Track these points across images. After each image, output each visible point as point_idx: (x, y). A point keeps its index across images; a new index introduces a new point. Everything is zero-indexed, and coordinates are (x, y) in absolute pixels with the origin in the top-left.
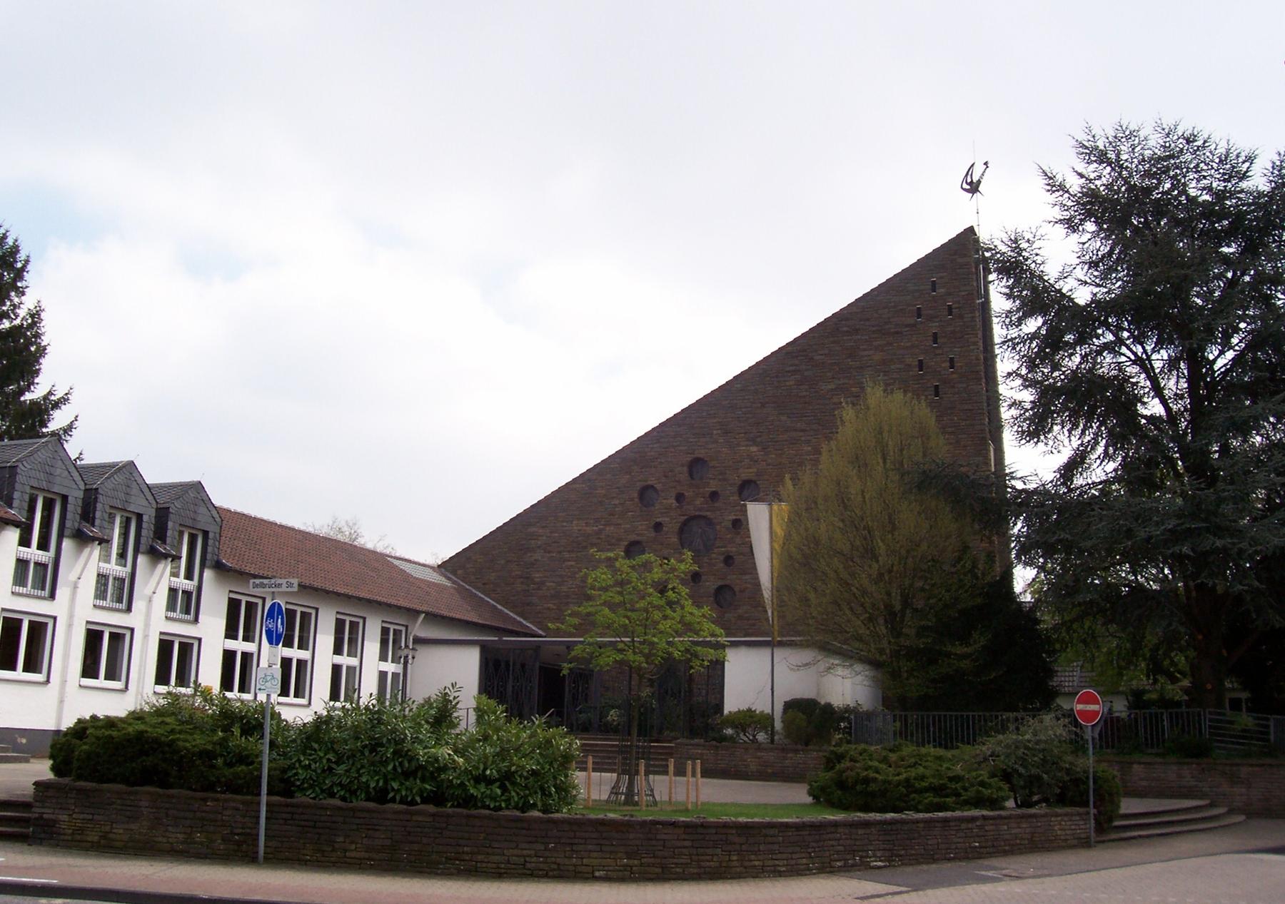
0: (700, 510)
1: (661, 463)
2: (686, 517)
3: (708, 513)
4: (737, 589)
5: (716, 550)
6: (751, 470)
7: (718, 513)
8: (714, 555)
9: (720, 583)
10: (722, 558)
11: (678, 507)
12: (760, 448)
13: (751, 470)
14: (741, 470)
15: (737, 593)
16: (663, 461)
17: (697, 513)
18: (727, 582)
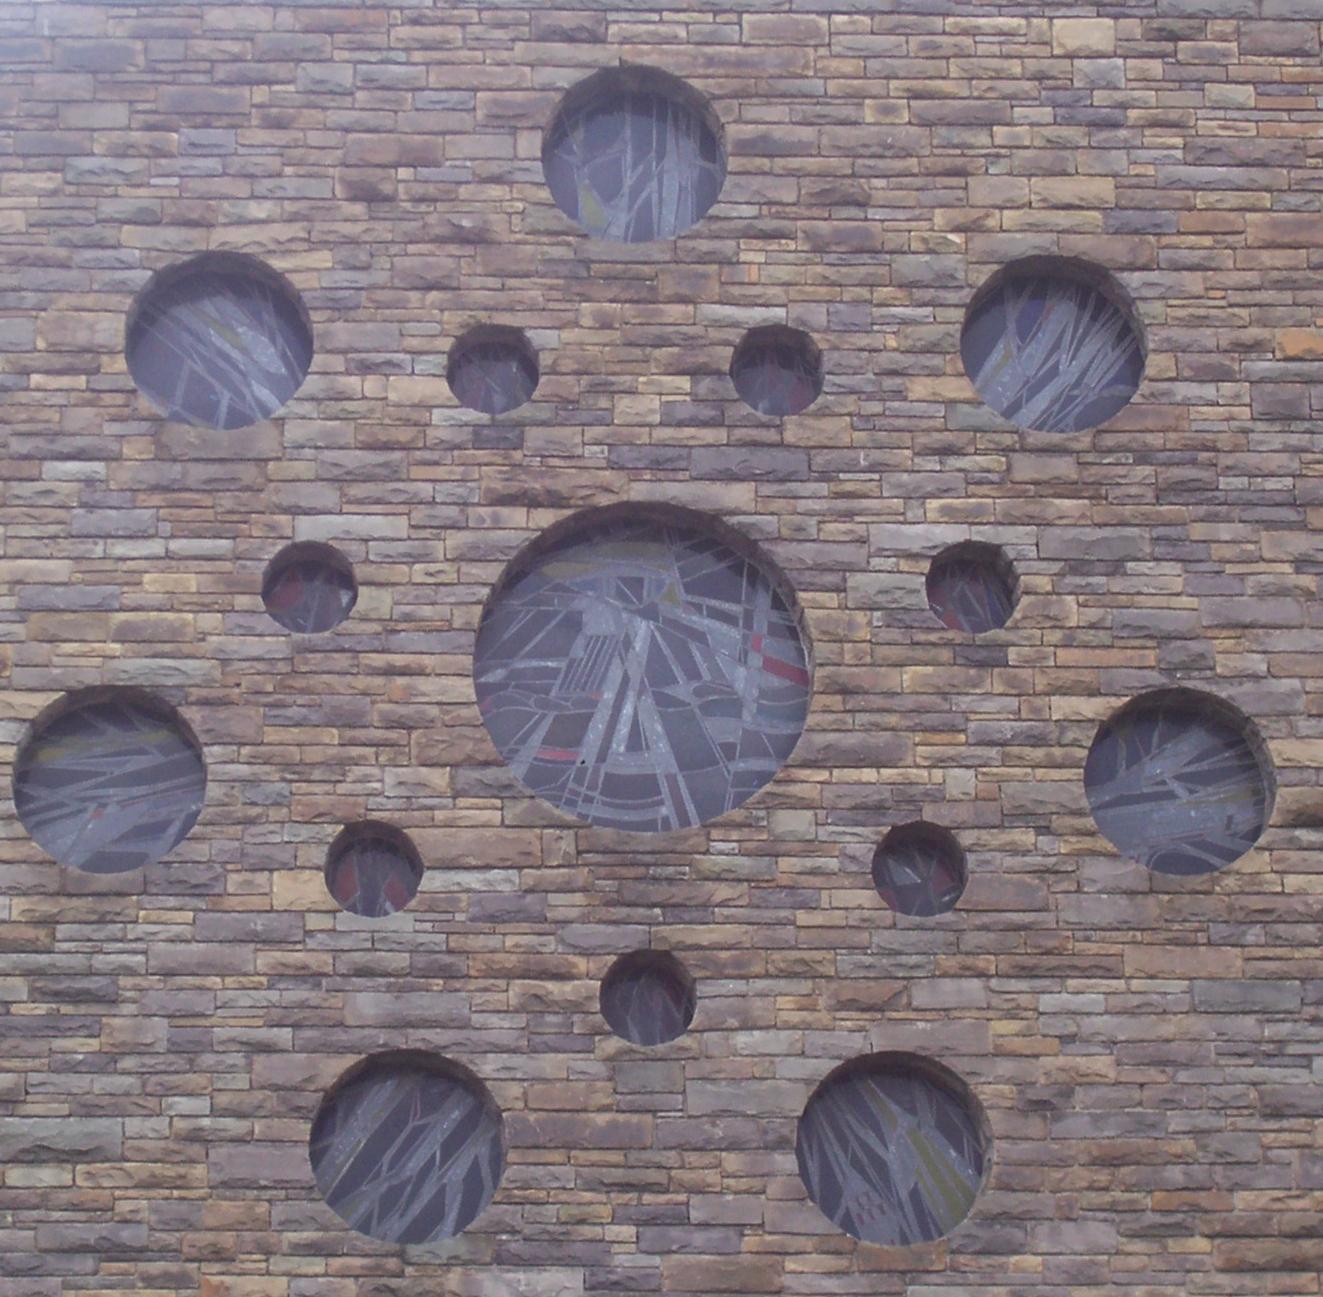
0: (662, 465)
1: (321, 94)
2: (545, 518)
3: (736, 496)
4: (992, 1090)
5: (810, 782)
6: (1064, 189)
7: (814, 496)
8: (793, 822)
9: (858, 1038)
10: (862, 842)
11: (479, 438)
12: (1133, 26)
13: (1064, 189)
14: (981, 190)
15: (996, 1121)
16: (345, 76)
17: (640, 491)
18: (911, 1035)
